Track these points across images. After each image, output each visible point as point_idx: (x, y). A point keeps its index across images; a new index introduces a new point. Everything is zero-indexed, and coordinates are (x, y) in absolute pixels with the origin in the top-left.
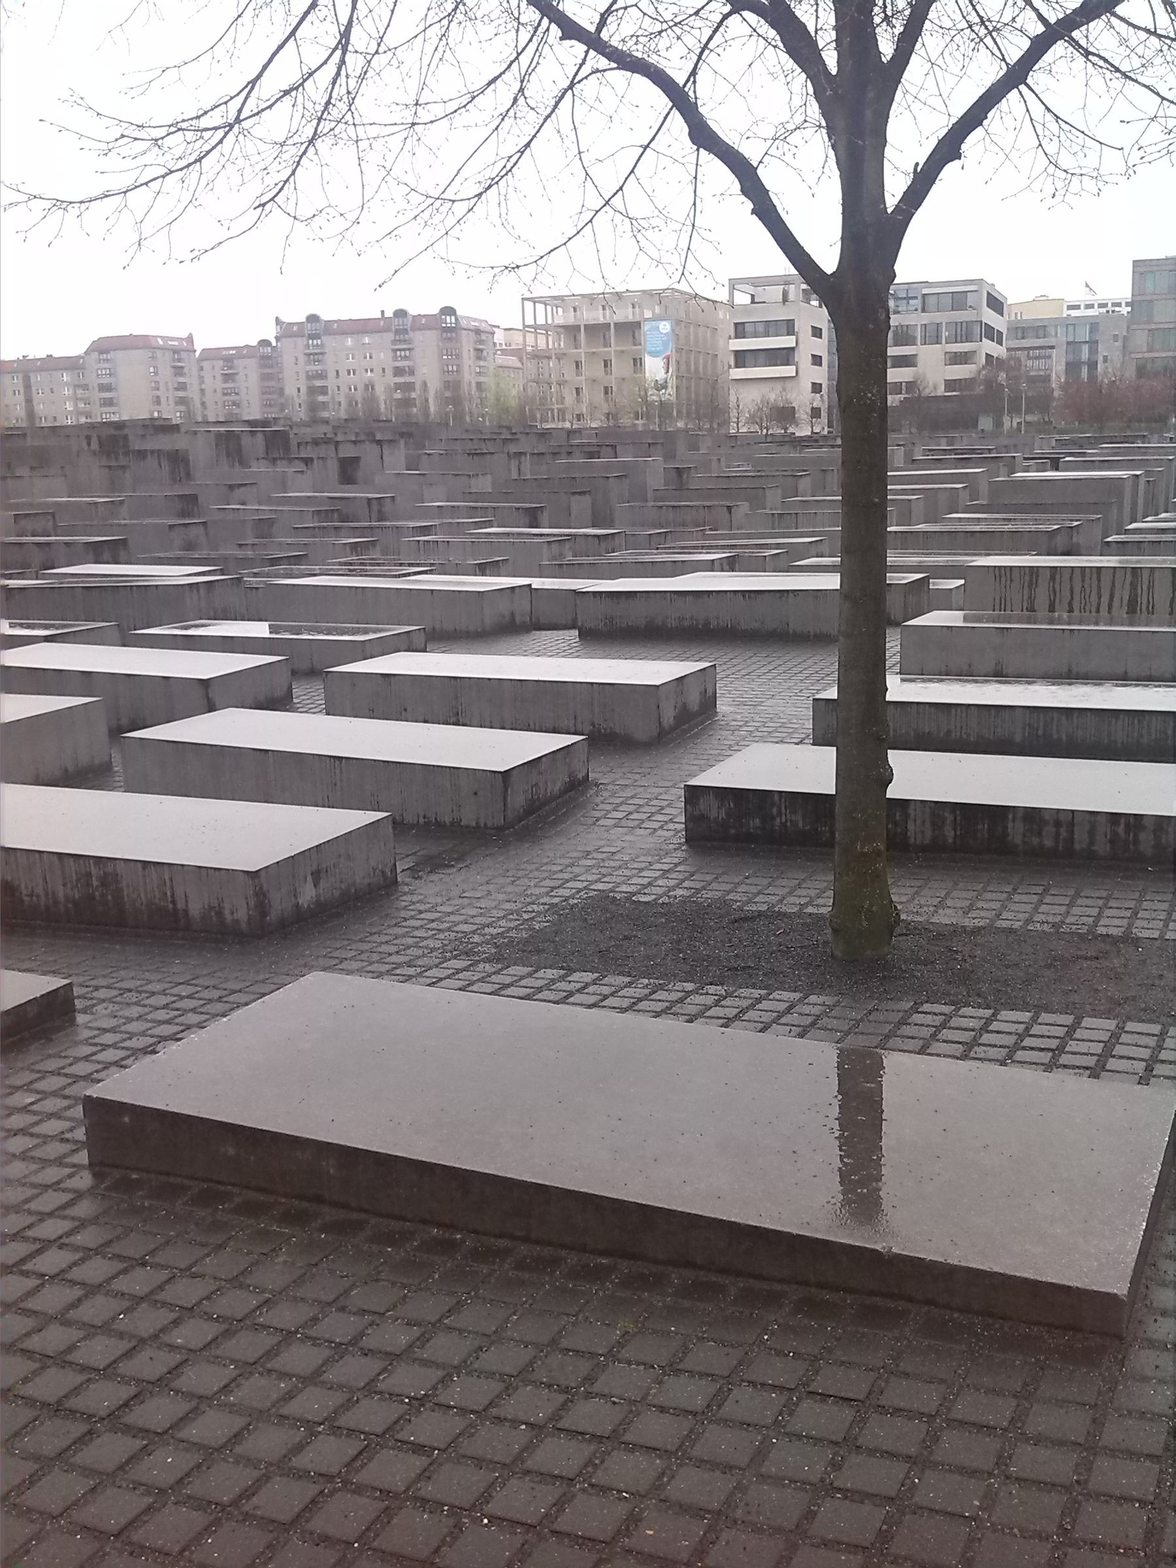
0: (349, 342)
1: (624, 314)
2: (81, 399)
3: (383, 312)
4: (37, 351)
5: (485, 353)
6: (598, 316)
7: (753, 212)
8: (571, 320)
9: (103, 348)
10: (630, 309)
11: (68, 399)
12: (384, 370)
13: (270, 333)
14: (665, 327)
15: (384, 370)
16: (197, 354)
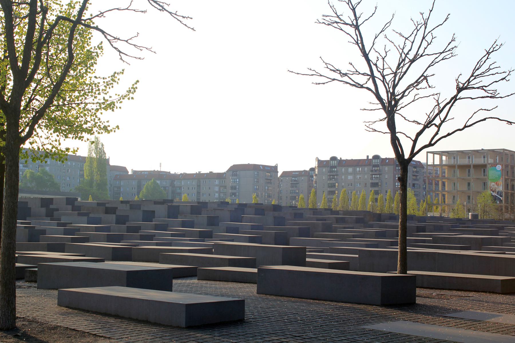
0: (350, 170)
1: (480, 161)
2: (222, 193)
3: (368, 156)
4: (205, 170)
5: (418, 177)
6: (465, 161)
7: (275, 169)
8: (452, 162)
9: (235, 170)
10: (483, 159)
11: (217, 192)
12: (366, 184)
13: (314, 164)
14: (499, 167)
15: (366, 184)
16: (279, 174)
